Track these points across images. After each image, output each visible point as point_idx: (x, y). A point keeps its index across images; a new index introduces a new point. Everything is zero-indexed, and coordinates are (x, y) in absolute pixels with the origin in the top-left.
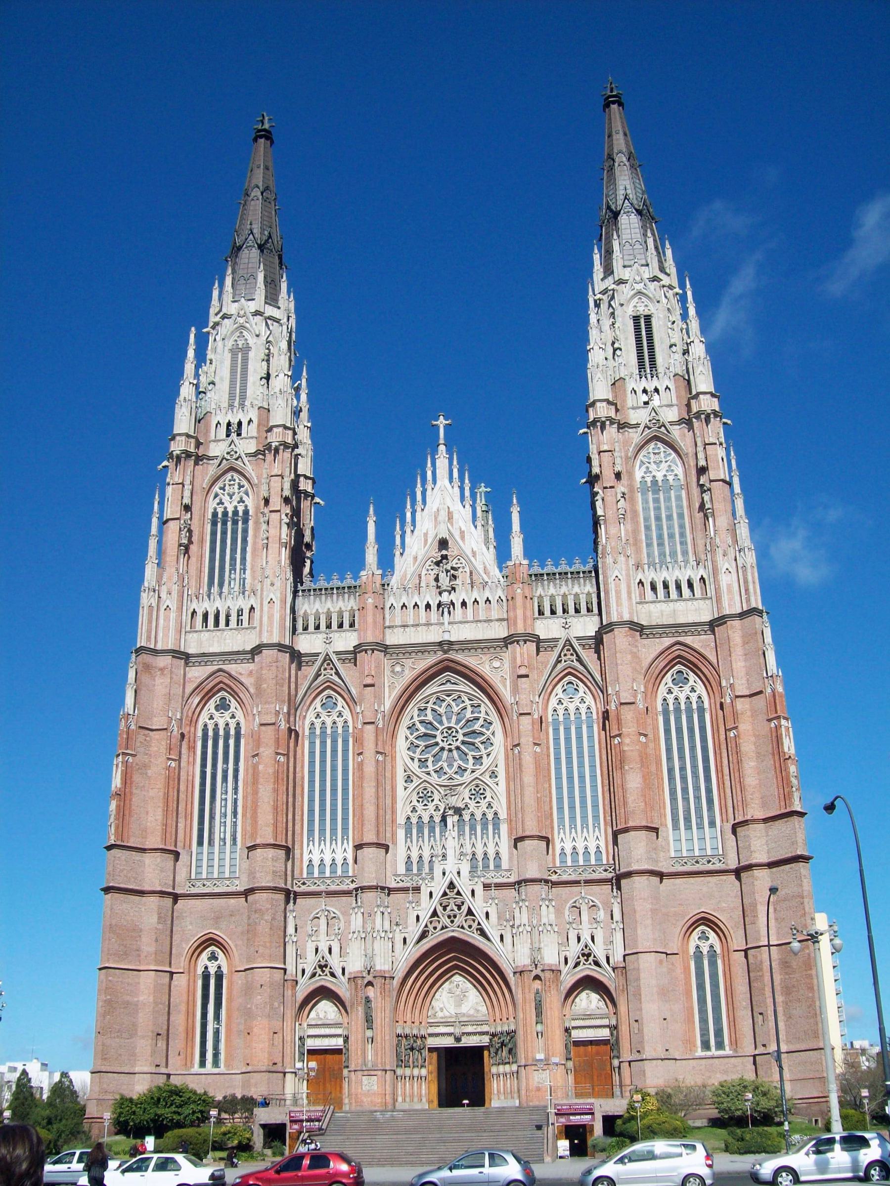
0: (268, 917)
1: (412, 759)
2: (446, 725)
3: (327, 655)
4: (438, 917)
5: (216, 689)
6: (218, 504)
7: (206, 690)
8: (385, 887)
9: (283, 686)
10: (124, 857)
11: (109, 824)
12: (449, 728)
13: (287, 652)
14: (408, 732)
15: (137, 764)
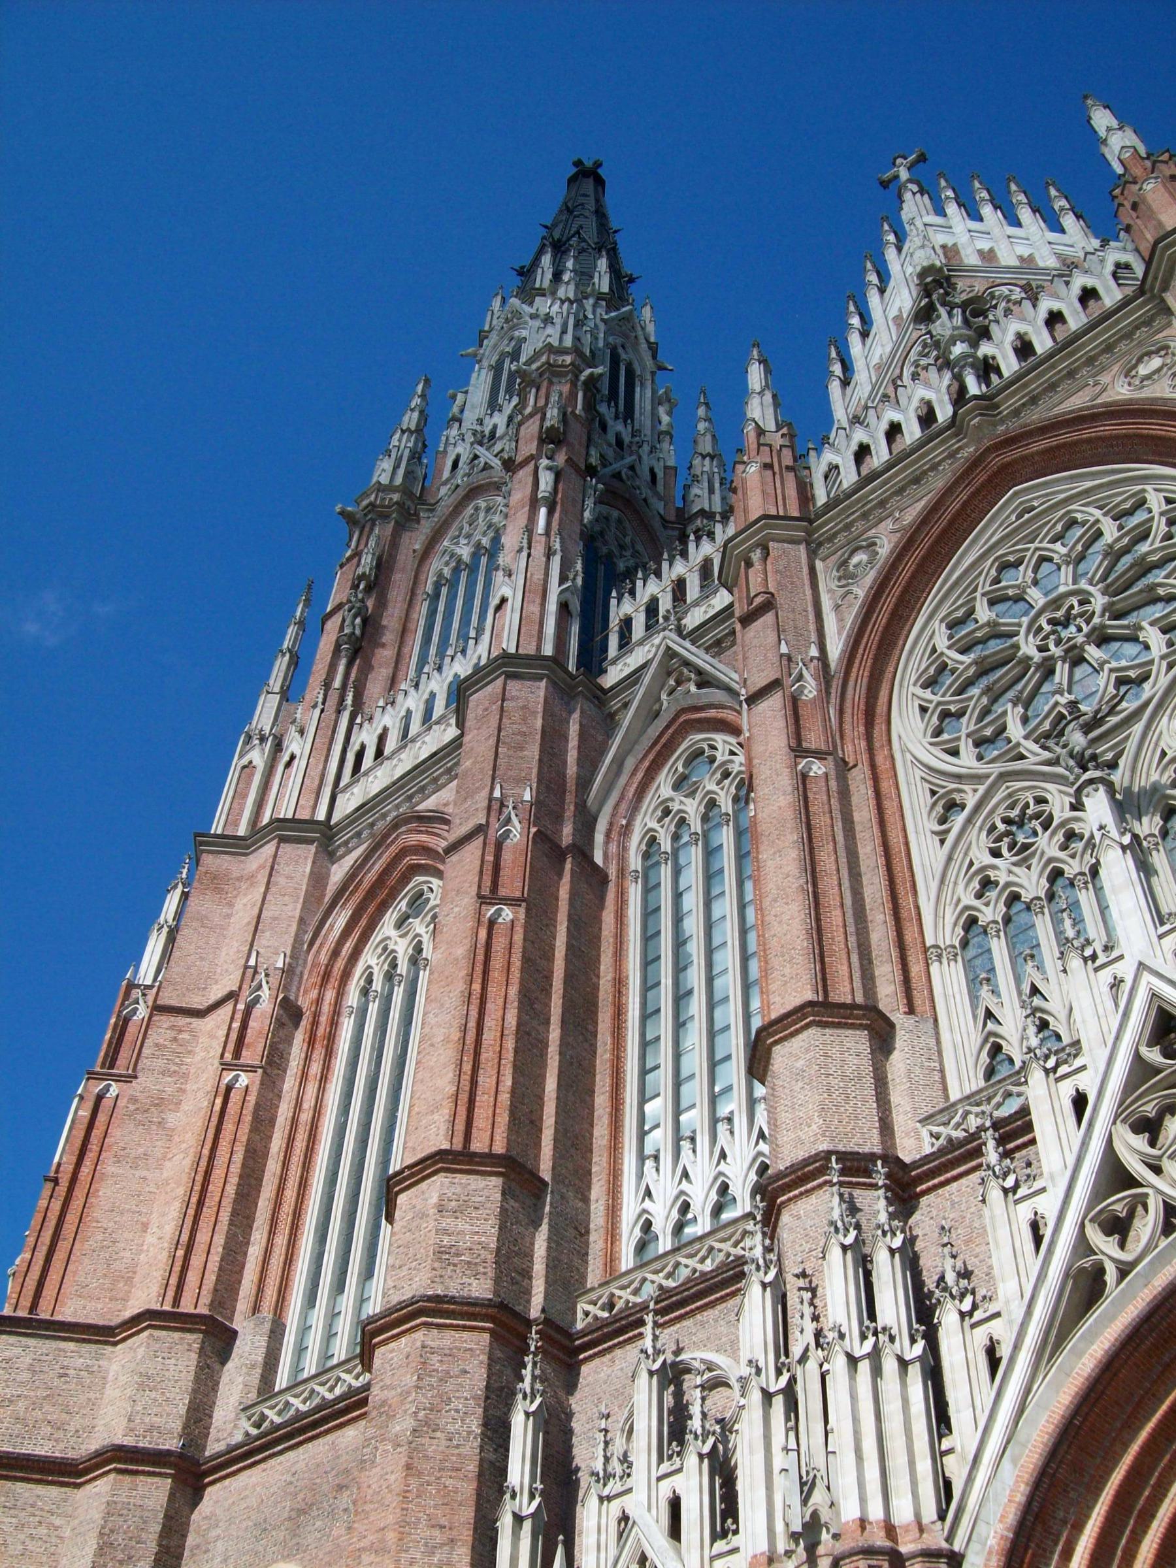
0: (402, 1425)
1: (955, 753)
2: (1042, 602)
3: (670, 653)
4: (1131, 1181)
5: (396, 874)
6: (447, 564)
7: (366, 885)
8: (872, 1157)
9: (522, 749)
10: (28, 1360)
11: (10, 1271)
12: (1055, 603)
13: (539, 678)
14: (927, 694)
15: (133, 1100)
